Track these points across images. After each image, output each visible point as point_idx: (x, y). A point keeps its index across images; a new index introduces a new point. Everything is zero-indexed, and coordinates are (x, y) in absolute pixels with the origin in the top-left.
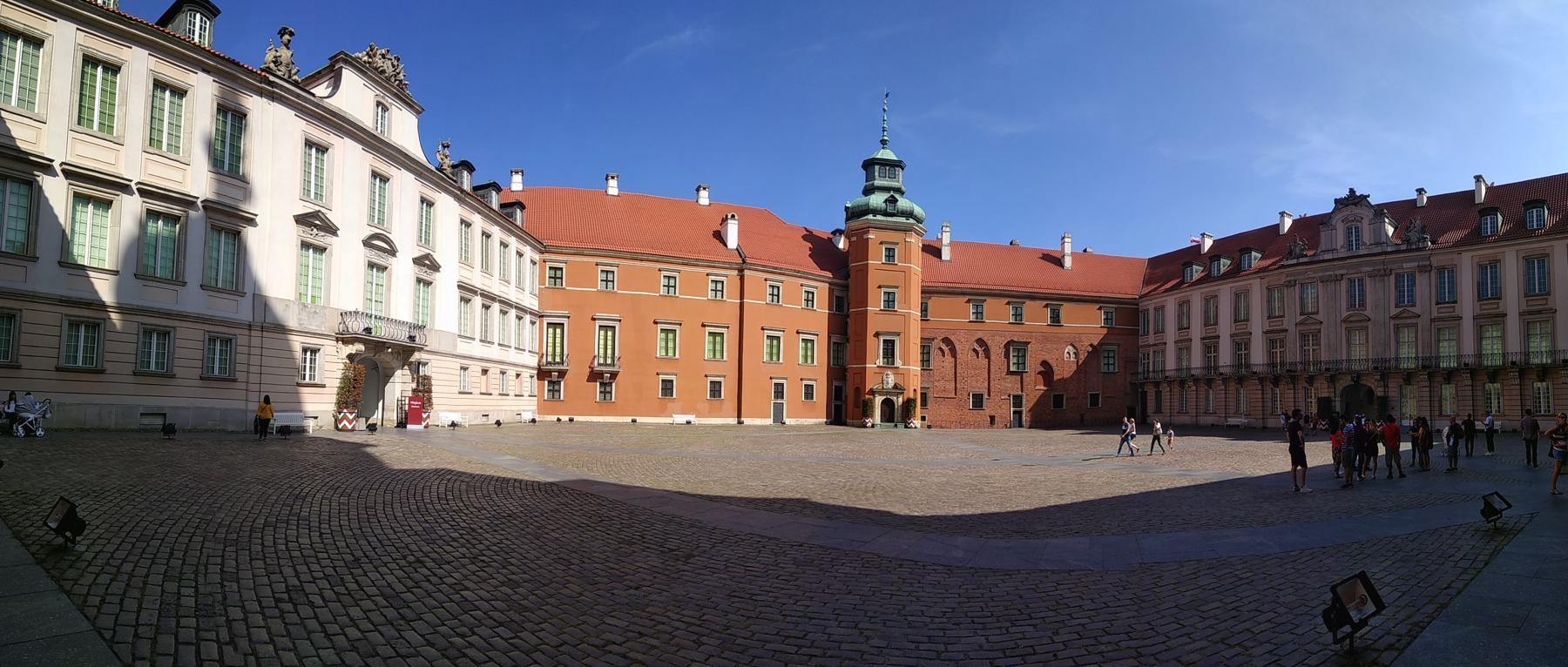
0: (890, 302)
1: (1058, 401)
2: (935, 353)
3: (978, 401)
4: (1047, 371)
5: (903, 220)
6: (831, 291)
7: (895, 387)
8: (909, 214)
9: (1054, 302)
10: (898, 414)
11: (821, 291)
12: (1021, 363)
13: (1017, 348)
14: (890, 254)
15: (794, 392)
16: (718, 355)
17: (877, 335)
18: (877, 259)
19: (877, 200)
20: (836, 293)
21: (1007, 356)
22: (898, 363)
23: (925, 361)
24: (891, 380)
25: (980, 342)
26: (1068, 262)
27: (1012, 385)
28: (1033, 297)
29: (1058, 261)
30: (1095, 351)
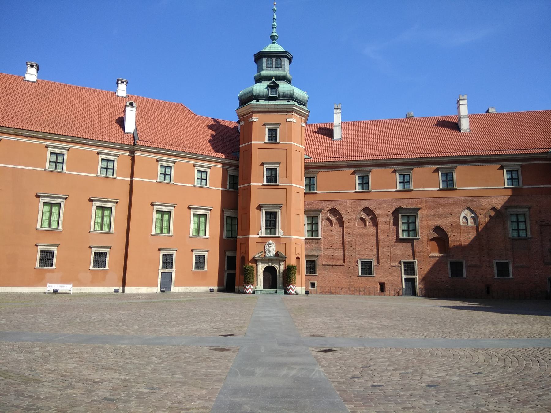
0: (272, 178)
1: (456, 268)
2: (322, 224)
3: (367, 268)
4: (441, 238)
5: (284, 102)
6: (225, 171)
7: (277, 255)
8: (290, 97)
9: (446, 166)
10: (280, 280)
11: (215, 171)
12: (412, 230)
13: (406, 215)
14: (273, 135)
15: (183, 263)
16: (106, 228)
17: (260, 207)
18: (259, 139)
19: (261, 88)
20: (231, 172)
21: (396, 223)
22: (280, 232)
23: (314, 230)
24: (272, 249)
25: (367, 210)
26: (465, 125)
27: (403, 253)
28: (421, 162)
29: (454, 126)
30: (499, 215)
